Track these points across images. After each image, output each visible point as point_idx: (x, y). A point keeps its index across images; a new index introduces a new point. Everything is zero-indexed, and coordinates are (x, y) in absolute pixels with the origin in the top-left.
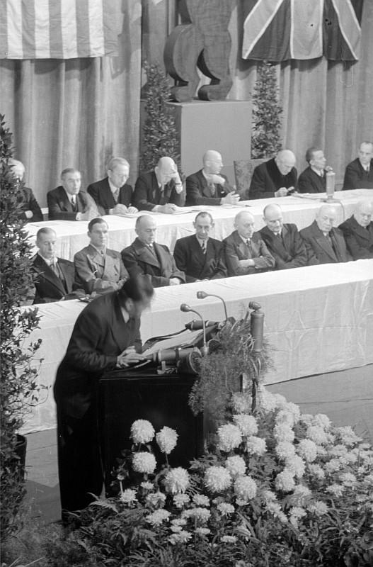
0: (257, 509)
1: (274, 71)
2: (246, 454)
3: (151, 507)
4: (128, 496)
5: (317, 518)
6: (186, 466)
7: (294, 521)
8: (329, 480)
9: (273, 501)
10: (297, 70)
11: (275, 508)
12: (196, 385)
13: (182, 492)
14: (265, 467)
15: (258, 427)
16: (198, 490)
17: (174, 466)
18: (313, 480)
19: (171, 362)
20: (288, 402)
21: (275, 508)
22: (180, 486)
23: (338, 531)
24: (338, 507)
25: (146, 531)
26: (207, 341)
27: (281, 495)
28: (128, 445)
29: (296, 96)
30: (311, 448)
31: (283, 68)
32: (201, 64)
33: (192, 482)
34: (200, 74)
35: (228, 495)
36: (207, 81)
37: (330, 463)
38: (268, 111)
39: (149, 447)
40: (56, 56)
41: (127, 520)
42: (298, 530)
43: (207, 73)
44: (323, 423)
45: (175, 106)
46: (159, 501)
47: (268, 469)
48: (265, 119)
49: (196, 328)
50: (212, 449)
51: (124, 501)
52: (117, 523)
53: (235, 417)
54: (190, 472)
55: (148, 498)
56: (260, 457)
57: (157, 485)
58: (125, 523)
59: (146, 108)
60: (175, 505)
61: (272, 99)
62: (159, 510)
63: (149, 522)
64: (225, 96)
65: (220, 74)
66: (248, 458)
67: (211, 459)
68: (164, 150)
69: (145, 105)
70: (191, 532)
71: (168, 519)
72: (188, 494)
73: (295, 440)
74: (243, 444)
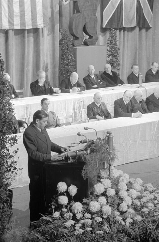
1: (116, 33)
10: (126, 32)
31: (120, 31)
32: (85, 30)
34: (84, 34)
36: (88, 37)
61: (115, 44)
65: (93, 34)
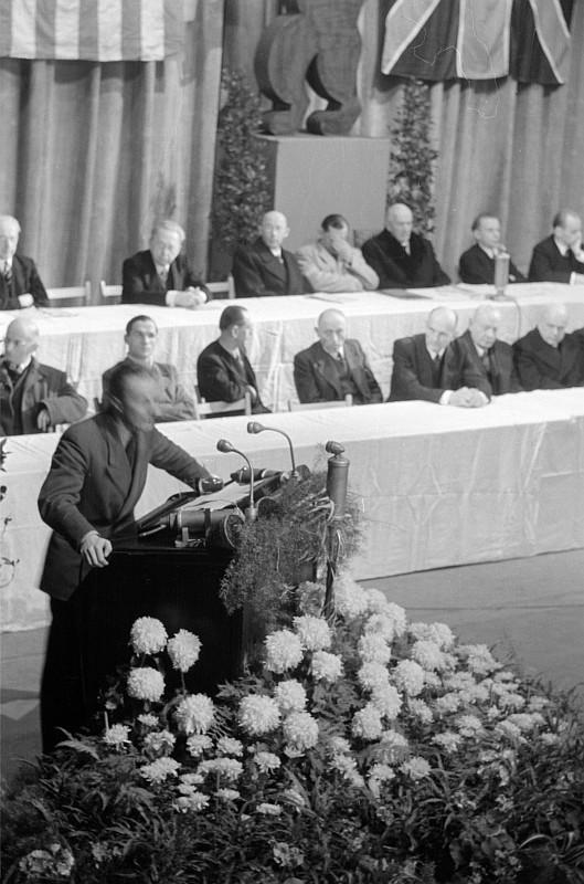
0: (317, 764)
1: (428, 95)
2: (311, 678)
3: (151, 754)
4: (117, 734)
5: (413, 783)
6: (211, 692)
7: (375, 786)
8: (440, 724)
9: (345, 754)
10: (470, 92)
11: (346, 764)
12: (232, 567)
13: (201, 733)
14: (339, 700)
15: (333, 638)
16: (226, 731)
17: (193, 691)
18: (413, 724)
19: (197, 530)
20: (389, 601)
21: (346, 764)
22: (199, 723)
23: (445, 805)
24: (447, 768)
25: (141, 791)
26: (255, 500)
27: (359, 744)
28: (126, 657)
29: (467, 136)
30: (414, 675)
31: (447, 88)
32: (313, 77)
33: (218, 717)
34: (312, 95)
35: (276, 740)
36: (324, 104)
37: (443, 699)
38: (415, 155)
39: (157, 660)
40: (87, 56)
41: (111, 772)
42: (379, 801)
43: (322, 92)
44: (441, 638)
45: (268, 142)
46: (165, 745)
47: (340, 703)
48: (410, 167)
49: (246, 481)
50: (257, 668)
51: (109, 741)
52: (96, 776)
53: (297, 620)
54: (217, 702)
55: (148, 740)
56: (332, 685)
57: (165, 720)
58: (110, 776)
59: (222, 142)
60: (189, 753)
61: (424, 137)
62: (163, 759)
63: (145, 776)
64: (349, 128)
65: (341, 94)
66: (313, 685)
67: (253, 683)
68: (247, 208)
69: (221, 137)
70: (209, 794)
71: (175, 773)
72: (211, 736)
73: (391, 661)
74: (306, 662)
